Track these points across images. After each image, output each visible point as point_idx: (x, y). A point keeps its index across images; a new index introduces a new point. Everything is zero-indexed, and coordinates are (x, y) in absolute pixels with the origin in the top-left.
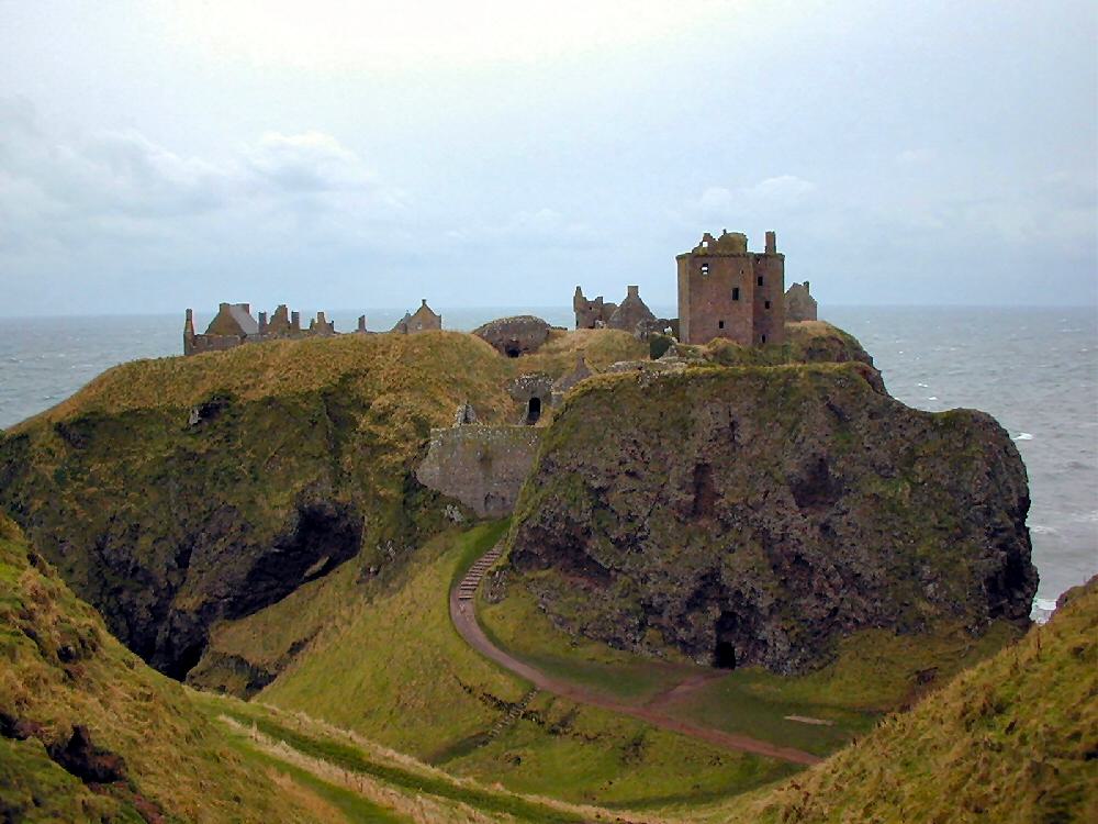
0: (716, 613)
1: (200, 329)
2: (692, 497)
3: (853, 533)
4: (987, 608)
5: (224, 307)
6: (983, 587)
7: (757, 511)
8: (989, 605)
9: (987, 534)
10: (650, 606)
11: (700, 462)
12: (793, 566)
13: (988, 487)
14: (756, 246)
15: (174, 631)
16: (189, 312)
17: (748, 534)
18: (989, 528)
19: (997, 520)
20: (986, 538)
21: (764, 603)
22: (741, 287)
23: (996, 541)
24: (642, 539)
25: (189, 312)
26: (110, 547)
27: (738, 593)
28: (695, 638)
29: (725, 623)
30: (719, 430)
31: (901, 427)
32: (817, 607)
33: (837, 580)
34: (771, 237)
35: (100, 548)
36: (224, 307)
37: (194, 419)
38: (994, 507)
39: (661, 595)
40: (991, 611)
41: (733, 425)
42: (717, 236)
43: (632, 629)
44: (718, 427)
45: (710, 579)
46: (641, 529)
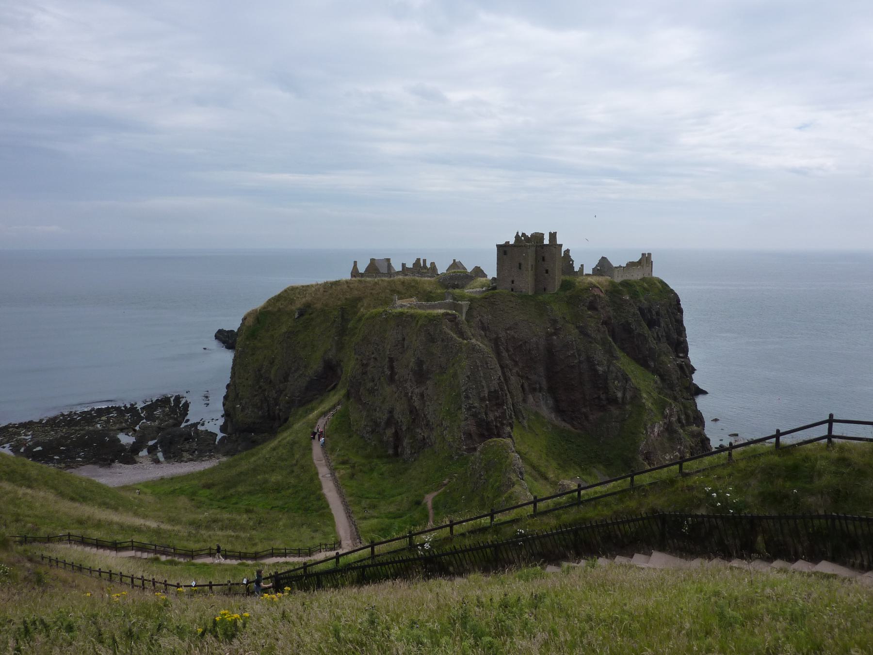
0: (394, 431)
1: (362, 269)
5: (372, 260)
12: (413, 411)
14: (546, 241)
15: (280, 410)
16: (355, 263)
21: (404, 428)
24: (377, 390)
25: (355, 263)
26: (264, 370)
34: (553, 236)
35: (259, 371)
36: (372, 260)
37: (296, 315)
41: (404, 339)
45: (391, 412)
46: (376, 385)
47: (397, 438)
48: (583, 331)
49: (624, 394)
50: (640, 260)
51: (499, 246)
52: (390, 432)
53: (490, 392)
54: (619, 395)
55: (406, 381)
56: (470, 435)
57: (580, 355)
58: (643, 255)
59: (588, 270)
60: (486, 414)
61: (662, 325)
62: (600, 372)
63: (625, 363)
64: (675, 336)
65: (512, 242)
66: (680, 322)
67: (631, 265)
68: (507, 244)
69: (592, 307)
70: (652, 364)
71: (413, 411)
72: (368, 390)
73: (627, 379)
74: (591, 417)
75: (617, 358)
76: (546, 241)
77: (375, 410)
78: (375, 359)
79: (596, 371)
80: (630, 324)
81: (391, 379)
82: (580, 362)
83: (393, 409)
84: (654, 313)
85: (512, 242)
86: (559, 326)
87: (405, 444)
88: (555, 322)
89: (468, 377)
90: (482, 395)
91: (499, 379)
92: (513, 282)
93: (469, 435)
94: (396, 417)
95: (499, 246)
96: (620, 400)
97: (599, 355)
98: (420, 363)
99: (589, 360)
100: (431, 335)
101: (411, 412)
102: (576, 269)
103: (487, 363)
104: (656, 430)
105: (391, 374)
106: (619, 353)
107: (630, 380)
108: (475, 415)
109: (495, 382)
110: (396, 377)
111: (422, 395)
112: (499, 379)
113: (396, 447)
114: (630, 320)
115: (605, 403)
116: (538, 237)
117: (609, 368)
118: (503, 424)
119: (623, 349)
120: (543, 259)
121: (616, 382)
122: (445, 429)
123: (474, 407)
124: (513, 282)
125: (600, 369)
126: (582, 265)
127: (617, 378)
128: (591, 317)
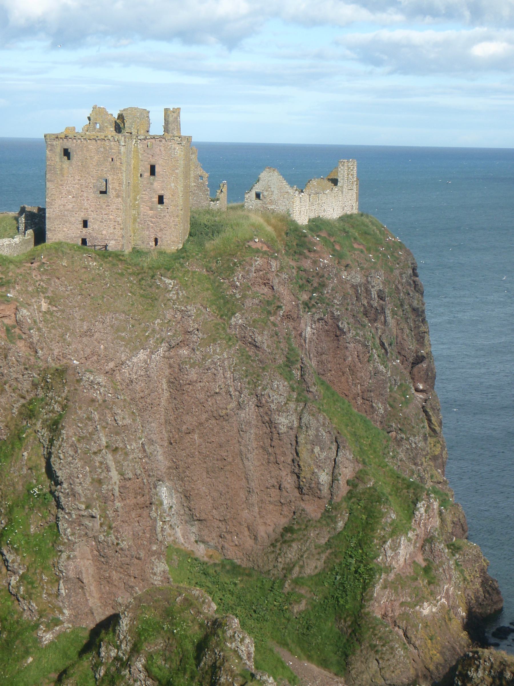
22: (110, 179)
62: (283, 429)
74: (262, 531)
76: (157, 128)
84: (374, 294)
92: (85, 224)
104: (402, 551)
121: (317, 449)
124: (85, 224)
125: (283, 421)
127: (317, 441)
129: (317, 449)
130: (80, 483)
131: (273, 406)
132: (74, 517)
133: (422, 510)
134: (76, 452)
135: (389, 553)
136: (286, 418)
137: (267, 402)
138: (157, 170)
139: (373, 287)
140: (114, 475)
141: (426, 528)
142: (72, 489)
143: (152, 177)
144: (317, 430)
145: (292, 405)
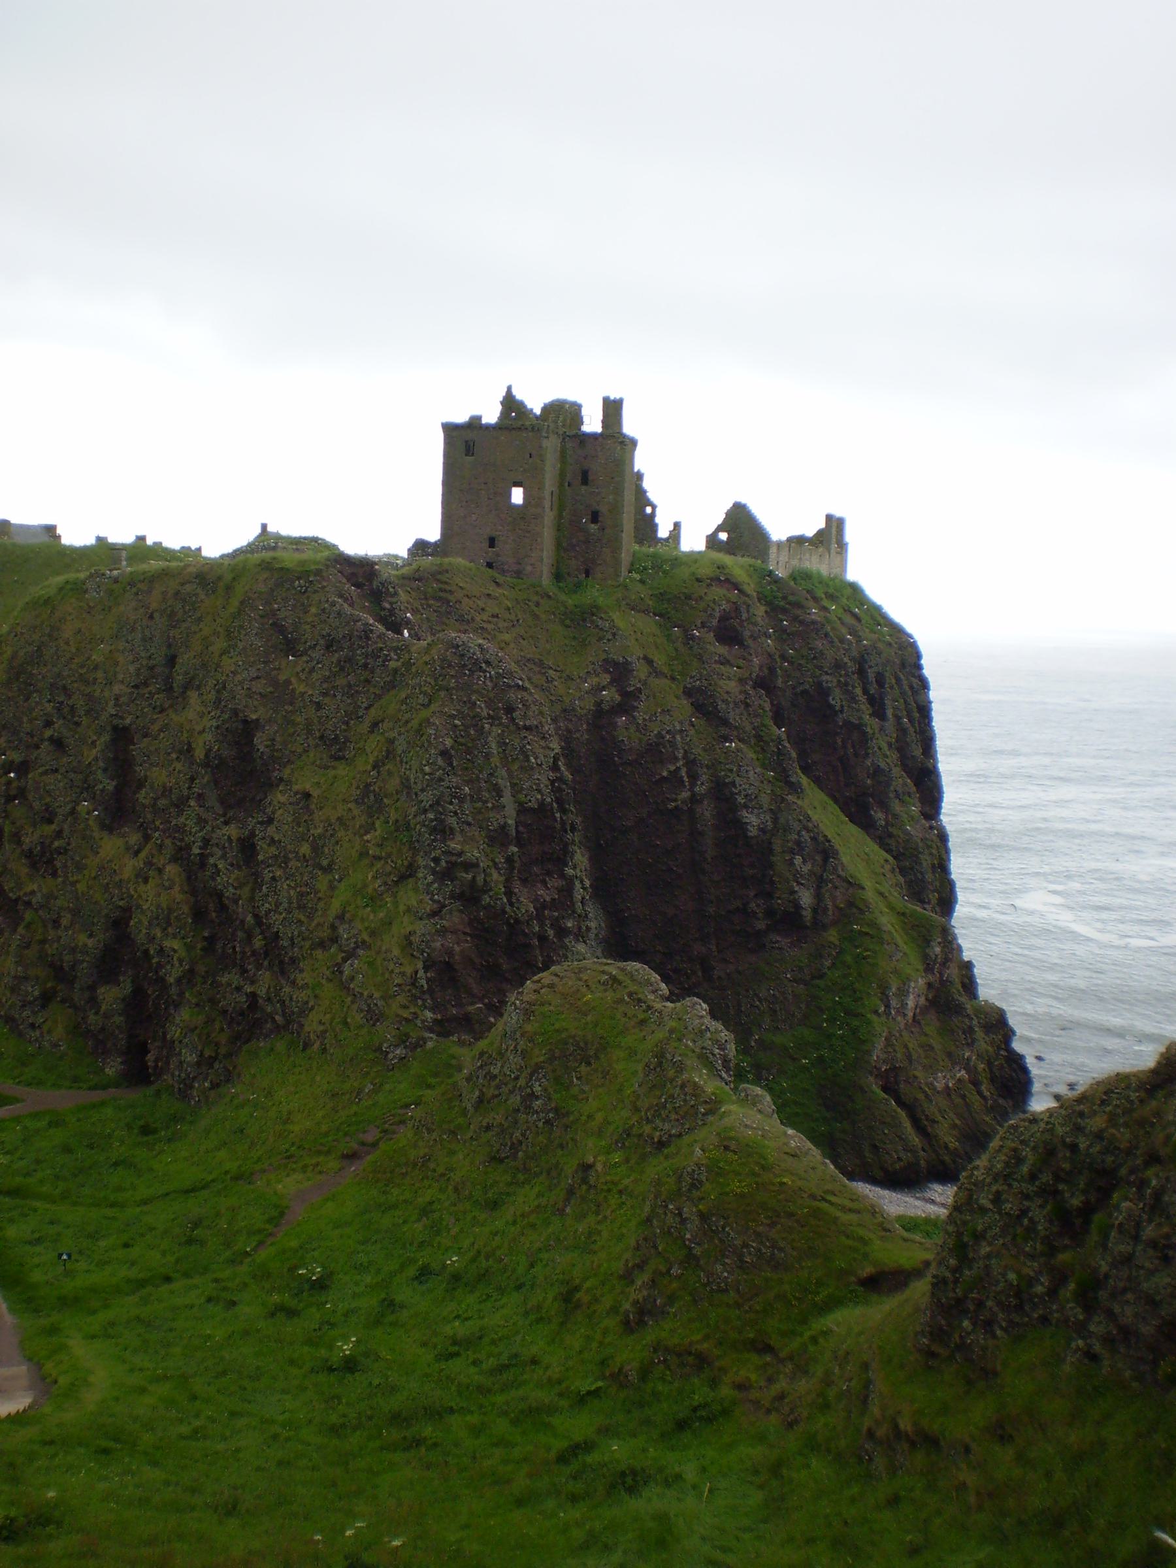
0: (126, 988)
2: (110, 785)
3: (275, 857)
4: (429, 1015)
6: (421, 973)
7: (181, 813)
8: (433, 1009)
9: (434, 873)
10: (61, 968)
11: (115, 722)
13: (441, 780)
14: (592, 423)
17: (169, 851)
18: (436, 860)
19: (454, 845)
20: (430, 878)
21: (172, 974)
23: (449, 886)
27: (146, 952)
28: (103, 1029)
29: (136, 1005)
30: (152, 668)
31: (365, 666)
32: (238, 989)
33: (258, 943)
34: (613, 409)
38: (452, 821)
39: (73, 950)
40: (435, 1021)
41: (172, 661)
42: (535, 405)
43: (30, 1003)
44: (152, 662)
45: (120, 924)
47: (144, 1012)
48: (704, 704)
49: (818, 896)
50: (820, 533)
51: (450, 430)
52: (111, 996)
53: (522, 810)
54: (806, 898)
55: (180, 805)
56: (449, 966)
57: (694, 777)
58: (829, 518)
59: (693, 542)
60: (509, 893)
61: (889, 713)
62: (753, 832)
63: (819, 810)
64: (918, 752)
65: (491, 415)
66: (924, 712)
67: (798, 542)
68: (474, 424)
69: (728, 634)
70: (879, 816)
71: (209, 911)
72: (29, 855)
73: (826, 853)
75: (795, 788)
76: (592, 423)
77: (56, 923)
78: (58, 744)
79: (741, 826)
80: (824, 692)
81: (119, 811)
82: (694, 799)
83: (127, 912)
85: (491, 415)
86: (633, 684)
87: (174, 1033)
88: (619, 671)
89: (444, 753)
90: (495, 820)
91: (555, 768)
92: (492, 542)
93: (444, 972)
94: (141, 938)
95: (450, 430)
96: (807, 914)
97: (751, 777)
98: (242, 732)
99: (722, 793)
100: (278, 628)
101: (199, 914)
102: (663, 532)
103: (510, 710)
104: (911, 1003)
105: (118, 790)
106: (804, 780)
107: (835, 854)
108: (470, 897)
109: (543, 777)
110: (144, 797)
111: (248, 847)
112: (555, 768)
113: (136, 1052)
114: (829, 681)
115: (761, 925)
116: (564, 414)
117: (775, 820)
118: (562, 932)
119: (806, 769)
120: (585, 479)
121: (798, 860)
122: (350, 955)
123: (469, 866)
124: (492, 542)
125: (753, 820)
126: (677, 526)
128: (724, 662)
129: (798, 860)
130: (456, 813)
131: (741, 800)
132: (443, 864)
133: (938, 950)
134: (451, 764)
135: (894, 1003)
136: (758, 816)
137: (733, 794)
138: (590, 478)
139: (870, 667)
140: (507, 799)
141: (941, 974)
142: (442, 821)
143: (583, 488)
144: (799, 833)
145: (765, 800)
